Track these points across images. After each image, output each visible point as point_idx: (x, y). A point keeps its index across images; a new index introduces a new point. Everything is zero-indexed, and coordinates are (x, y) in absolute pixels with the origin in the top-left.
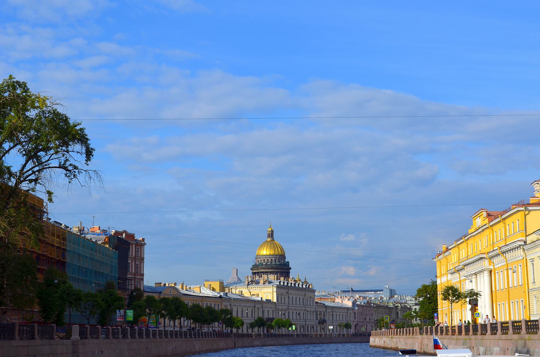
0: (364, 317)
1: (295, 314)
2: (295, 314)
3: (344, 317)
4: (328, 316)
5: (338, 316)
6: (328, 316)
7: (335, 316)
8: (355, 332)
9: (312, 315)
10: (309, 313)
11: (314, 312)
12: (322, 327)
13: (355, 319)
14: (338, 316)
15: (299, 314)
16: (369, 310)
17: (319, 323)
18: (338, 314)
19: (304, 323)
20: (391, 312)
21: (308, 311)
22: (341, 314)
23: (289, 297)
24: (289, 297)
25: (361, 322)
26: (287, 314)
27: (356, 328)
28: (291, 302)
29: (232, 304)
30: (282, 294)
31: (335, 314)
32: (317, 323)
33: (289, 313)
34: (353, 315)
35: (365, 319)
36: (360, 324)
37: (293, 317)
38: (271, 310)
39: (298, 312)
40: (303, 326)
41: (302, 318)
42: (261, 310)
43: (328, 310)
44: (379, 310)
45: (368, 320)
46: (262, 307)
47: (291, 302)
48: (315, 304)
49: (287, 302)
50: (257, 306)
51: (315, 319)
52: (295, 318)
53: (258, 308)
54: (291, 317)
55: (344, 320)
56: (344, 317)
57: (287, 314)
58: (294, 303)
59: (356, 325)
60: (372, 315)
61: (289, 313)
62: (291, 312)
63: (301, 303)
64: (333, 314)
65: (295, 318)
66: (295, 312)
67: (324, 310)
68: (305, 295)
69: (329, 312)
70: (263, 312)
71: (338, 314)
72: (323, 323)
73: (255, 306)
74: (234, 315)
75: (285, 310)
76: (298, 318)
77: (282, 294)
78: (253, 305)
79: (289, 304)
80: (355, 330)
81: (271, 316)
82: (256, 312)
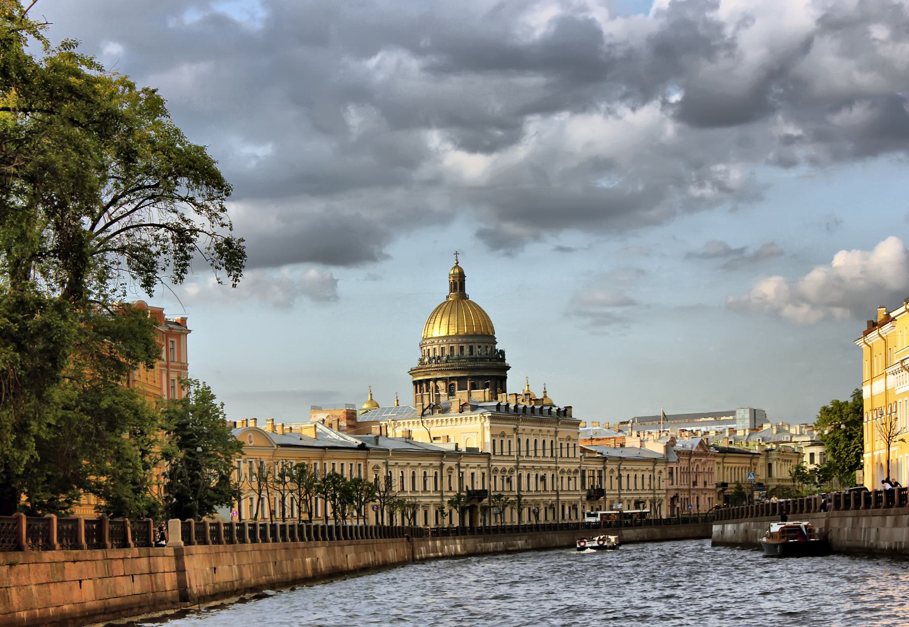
0: (693, 478)
4: (608, 479)
7: (624, 480)
11: (576, 471)
20: (755, 464)
31: (624, 474)
32: (584, 498)
34: (665, 475)
35: (695, 483)
41: (549, 488)
44: (726, 460)
45: (700, 485)
48: (579, 454)
59: (672, 500)
60: (711, 472)
71: (632, 474)
72: (598, 498)
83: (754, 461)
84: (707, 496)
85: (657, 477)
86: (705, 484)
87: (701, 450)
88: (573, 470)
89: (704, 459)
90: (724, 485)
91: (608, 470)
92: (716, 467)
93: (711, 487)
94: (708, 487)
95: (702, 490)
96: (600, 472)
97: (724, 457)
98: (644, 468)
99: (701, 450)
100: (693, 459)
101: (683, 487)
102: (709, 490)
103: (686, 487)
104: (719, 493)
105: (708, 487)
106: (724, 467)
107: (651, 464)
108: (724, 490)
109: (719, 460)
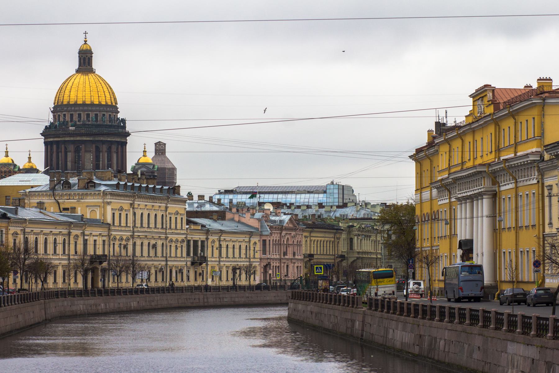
0: (283, 249)
1: (145, 248)
2: (145, 248)
3: (243, 252)
4: (210, 249)
5: (230, 250)
6: (210, 249)
7: (224, 250)
8: (265, 281)
9: (179, 249)
10: (173, 245)
11: (183, 241)
12: (199, 271)
13: (264, 252)
14: (230, 250)
15: (154, 246)
16: (294, 237)
17: (193, 263)
18: (231, 245)
19: (163, 263)
21: (171, 241)
23: (134, 214)
24: (134, 214)
25: (276, 259)
26: (130, 248)
27: (265, 272)
28: (138, 224)
29: (28, 230)
30: (121, 209)
31: (224, 244)
32: (189, 263)
33: (134, 245)
35: (285, 254)
36: (274, 264)
37: (143, 254)
38: (100, 240)
39: (153, 242)
40: (161, 270)
41: (159, 253)
42: (80, 241)
43: (211, 238)
44: (312, 234)
45: (290, 256)
46: (83, 234)
47: (138, 224)
48: (185, 226)
49: (130, 224)
50: (74, 232)
51: (185, 254)
52: (145, 254)
53: (77, 236)
54: (138, 253)
56: (243, 252)
57: (130, 248)
58: (145, 224)
59: (265, 267)
60: (299, 245)
61: (134, 245)
62: (138, 242)
63: (159, 225)
64: (220, 245)
65: (145, 254)
66: (146, 242)
67: (203, 237)
68: (167, 208)
69: (213, 241)
71: (231, 245)
72: (201, 264)
73: (69, 234)
75: (128, 240)
76: (152, 253)
77: (121, 209)
78: (65, 231)
79: (134, 226)
80: (265, 276)
81: (100, 252)
82: (72, 247)
83: (338, 235)
84: (296, 265)
86: (294, 254)
87: (291, 226)
88: (180, 240)
89: (293, 233)
90: (311, 256)
93: (299, 257)
94: (296, 257)
95: (291, 259)
96: (203, 242)
97: (311, 232)
98: (241, 239)
99: (291, 226)
101: (275, 257)
102: (298, 260)
103: (278, 257)
104: (306, 263)
105: (296, 257)
106: (311, 241)
107: (248, 236)
108: (310, 260)
109: (307, 234)
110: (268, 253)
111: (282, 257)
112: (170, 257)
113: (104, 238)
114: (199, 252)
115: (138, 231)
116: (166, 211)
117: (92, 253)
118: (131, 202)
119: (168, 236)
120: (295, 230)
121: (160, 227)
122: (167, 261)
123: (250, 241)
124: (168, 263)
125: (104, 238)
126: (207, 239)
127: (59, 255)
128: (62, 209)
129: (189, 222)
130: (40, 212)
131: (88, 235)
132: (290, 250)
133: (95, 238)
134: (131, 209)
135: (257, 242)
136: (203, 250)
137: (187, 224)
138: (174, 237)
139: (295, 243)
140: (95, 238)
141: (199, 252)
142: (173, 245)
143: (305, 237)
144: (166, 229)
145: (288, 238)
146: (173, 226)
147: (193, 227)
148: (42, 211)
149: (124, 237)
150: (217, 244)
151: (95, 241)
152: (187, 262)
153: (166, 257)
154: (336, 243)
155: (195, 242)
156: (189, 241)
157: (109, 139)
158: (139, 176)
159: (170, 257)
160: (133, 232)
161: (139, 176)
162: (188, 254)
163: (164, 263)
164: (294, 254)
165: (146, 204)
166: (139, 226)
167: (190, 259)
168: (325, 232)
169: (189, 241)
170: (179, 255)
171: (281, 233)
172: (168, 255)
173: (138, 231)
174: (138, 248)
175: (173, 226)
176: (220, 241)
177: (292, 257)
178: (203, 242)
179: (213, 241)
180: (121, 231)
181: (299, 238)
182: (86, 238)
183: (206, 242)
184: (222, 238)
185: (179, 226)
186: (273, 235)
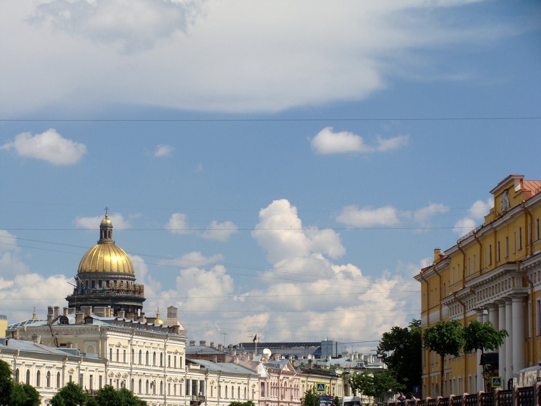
3: (242, 392)
10: (172, 384)
11: (182, 380)
13: (263, 395)
15: (153, 384)
18: (230, 386)
19: (162, 401)
21: (171, 379)
22: (236, 386)
25: (274, 402)
28: (136, 361)
31: (223, 385)
34: (258, 388)
39: (151, 380)
46: (79, 367)
52: (144, 391)
55: (242, 397)
56: (242, 392)
60: (297, 389)
63: (158, 363)
64: (220, 387)
65: (144, 391)
70: (81, 377)
71: (230, 386)
73: (63, 368)
74: (22, 379)
75: (126, 376)
76: (151, 391)
79: (132, 363)
83: (333, 382)
85: (251, 389)
86: (292, 398)
88: (179, 379)
89: (291, 378)
91: (209, 381)
92: (301, 384)
94: (294, 400)
95: (289, 403)
96: (202, 382)
100: (281, 377)
101: (273, 399)
103: (276, 400)
110: (266, 394)
111: (280, 400)
112: (169, 395)
113: (101, 374)
114: (199, 391)
115: (136, 368)
116: (165, 349)
117: (88, 388)
118: (130, 339)
119: (167, 374)
120: (293, 374)
121: (159, 365)
122: (165, 399)
123: (248, 384)
124: (167, 401)
125: (101, 374)
126: (206, 379)
127: (52, 388)
128: (59, 345)
129: (188, 362)
130: (34, 345)
131: (84, 370)
132: (288, 394)
133: (91, 373)
134: (129, 345)
135: (256, 384)
136: (202, 389)
137: (186, 364)
138: (173, 376)
139: (293, 387)
140: (91, 373)
141: (199, 391)
142: (172, 384)
143: (302, 381)
144: (165, 367)
145: (286, 383)
146: (172, 365)
147: (192, 367)
148: (36, 343)
149: (122, 374)
150: (216, 384)
151: (91, 376)
152: (185, 400)
153: (165, 395)
154: (332, 389)
155: (194, 382)
156: (188, 381)
157: (126, 304)
158: (139, 315)
159: (169, 395)
160: (131, 369)
161: (139, 315)
162: (187, 393)
163: (163, 401)
164: (292, 398)
165: (145, 341)
166: (138, 363)
167: (189, 398)
168: (321, 378)
169: (188, 381)
170: (178, 393)
171: (278, 377)
172: (167, 393)
173: (136, 368)
174: (136, 384)
175: (172, 365)
176: (219, 382)
177: (290, 401)
178: (202, 382)
179: (213, 382)
180: (118, 367)
181: (296, 382)
182: (81, 372)
183: (205, 382)
184: (221, 379)
185: (178, 365)
186: (271, 378)
